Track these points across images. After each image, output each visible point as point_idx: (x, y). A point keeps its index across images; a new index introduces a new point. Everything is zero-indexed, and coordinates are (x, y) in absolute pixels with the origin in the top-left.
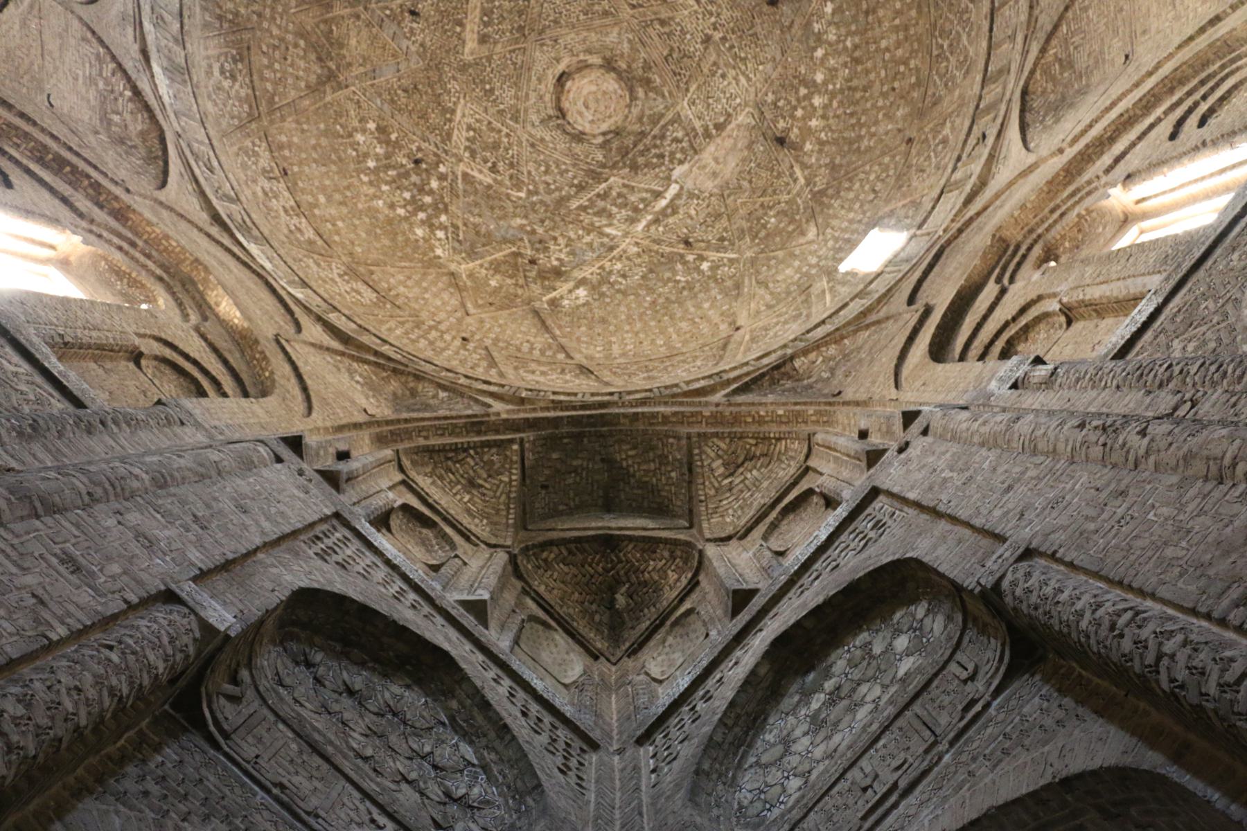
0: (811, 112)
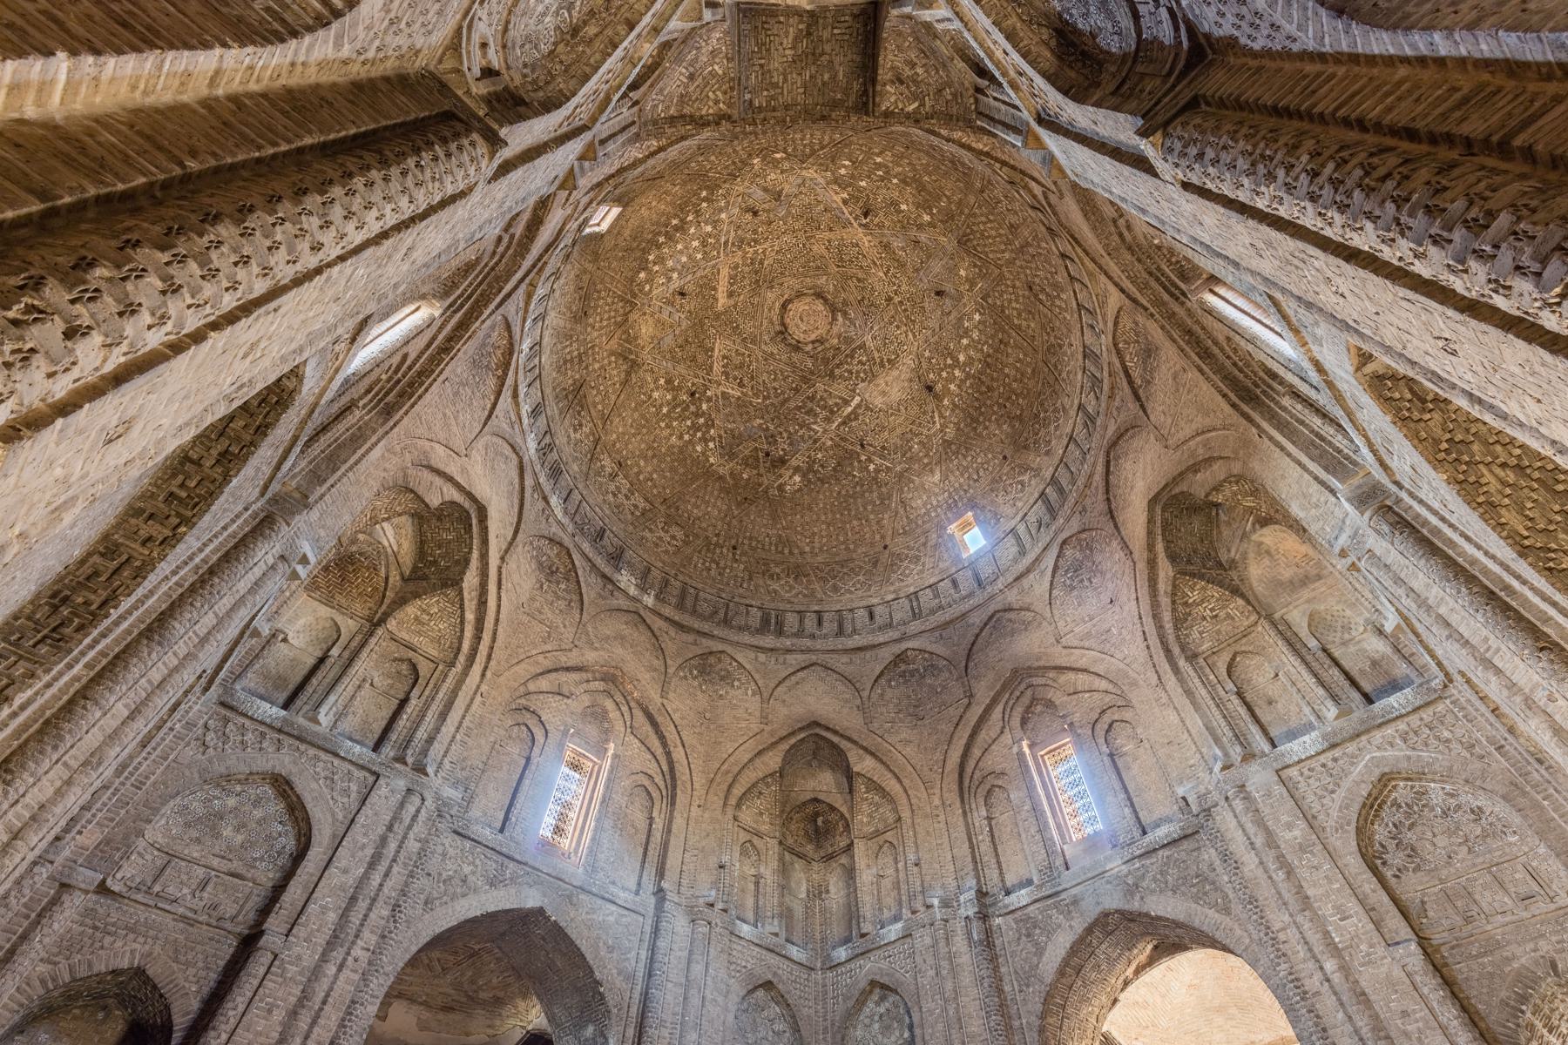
0: (951, 379)
